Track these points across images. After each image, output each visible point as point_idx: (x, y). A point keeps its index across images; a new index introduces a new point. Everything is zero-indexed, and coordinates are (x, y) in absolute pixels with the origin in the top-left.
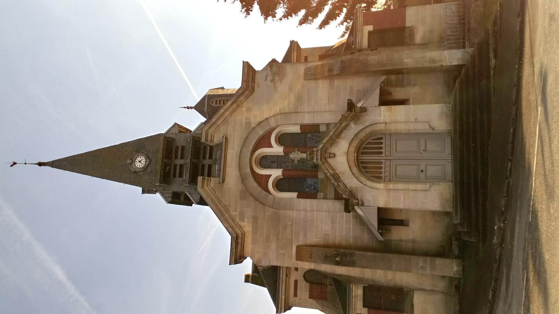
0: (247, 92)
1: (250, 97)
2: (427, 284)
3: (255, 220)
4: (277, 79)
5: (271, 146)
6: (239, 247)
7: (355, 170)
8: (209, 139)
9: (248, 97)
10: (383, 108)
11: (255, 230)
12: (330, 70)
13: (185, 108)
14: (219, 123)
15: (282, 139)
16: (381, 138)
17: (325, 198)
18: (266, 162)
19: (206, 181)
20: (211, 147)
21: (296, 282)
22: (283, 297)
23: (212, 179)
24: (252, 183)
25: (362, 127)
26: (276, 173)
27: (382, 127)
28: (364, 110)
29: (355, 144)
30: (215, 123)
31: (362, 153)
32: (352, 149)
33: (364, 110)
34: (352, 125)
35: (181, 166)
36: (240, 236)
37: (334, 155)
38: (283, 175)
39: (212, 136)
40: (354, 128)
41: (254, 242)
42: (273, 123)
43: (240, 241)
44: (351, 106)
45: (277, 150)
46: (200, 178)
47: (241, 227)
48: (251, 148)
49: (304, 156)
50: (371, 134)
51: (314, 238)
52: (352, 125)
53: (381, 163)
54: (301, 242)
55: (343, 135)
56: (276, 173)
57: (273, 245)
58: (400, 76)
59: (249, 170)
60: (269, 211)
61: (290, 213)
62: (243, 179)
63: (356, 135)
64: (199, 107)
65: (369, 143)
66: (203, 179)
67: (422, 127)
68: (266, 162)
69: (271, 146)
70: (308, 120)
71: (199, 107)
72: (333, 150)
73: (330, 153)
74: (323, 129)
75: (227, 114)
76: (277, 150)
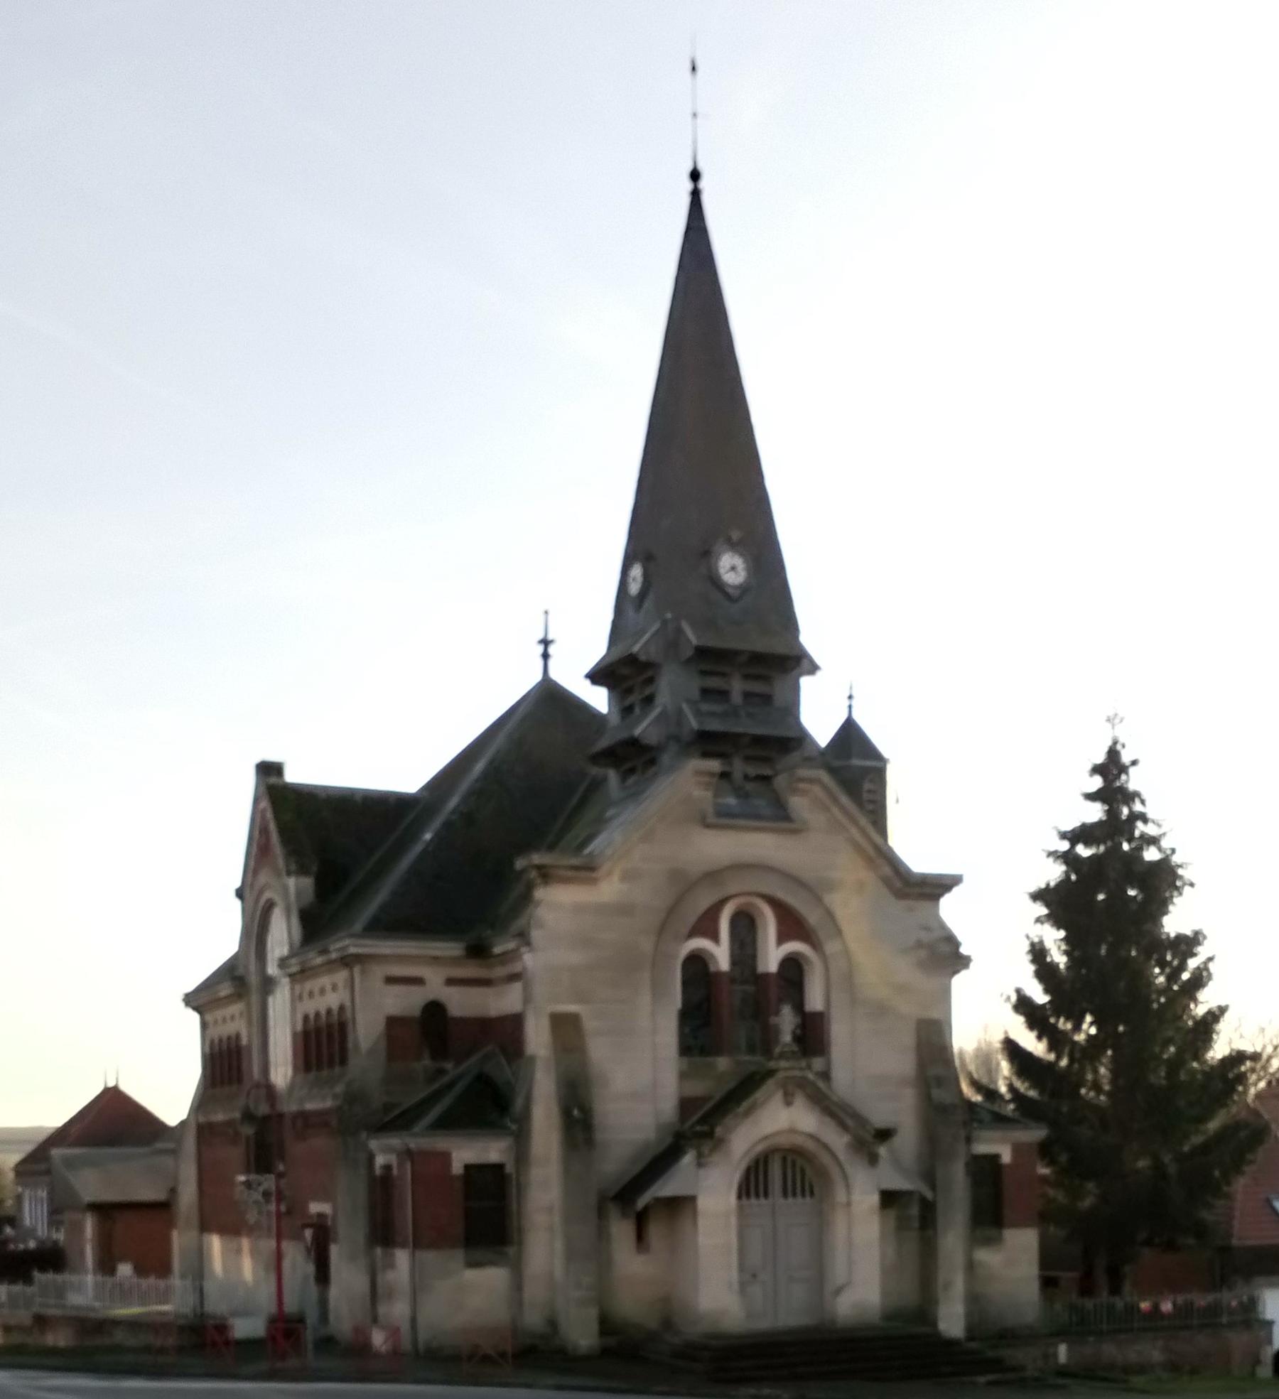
0: (898, 884)
1: (885, 891)
2: (534, 1292)
3: (623, 909)
4: (923, 953)
5: (781, 939)
6: (570, 873)
7: (760, 1148)
8: (801, 786)
9: (886, 882)
10: (875, 1199)
11: (602, 910)
12: (940, 1081)
13: (851, 688)
14: (835, 810)
15: (793, 969)
16: (812, 1193)
17: (683, 1076)
18: (745, 925)
19: (707, 779)
20: (766, 779)
21: (418, 981)
22: (387, 951)
23: (709, 794)
24: (703, 901)
25: (842, 1156)
26: (721, 955)
27: (841, 1196)
28: (873, 1160)
29: (810, 1145)
30: (835, 800)
31: (784, 1159)
32: (799, 1140)
33: (873, 1160)
34: (846, 1139)
35: (723, 695)
36: (594, 875)
37: (788, 1103)
38: (719, 974)
39: (804, 793)
40: (838, 1141)
41: (579, 909)
42: (831, 947)
43: (583, 874)
44: (885, 1135)
45: (772, 956)
46: (715, 765)
47: (609, 873)
48: (781, 895)
49: (787, 1037)
50: (823, 1174)
51: (599, 1050)
52: (846, 1139)
53: (766, 1195)
54: (589, 1024)
55: (828, 1119)
56: (721, 955)
57: (575, 957)
58: (916, 1224)
59: (732, 889)
60: (647, 945)
61: (645, 999)
62: (713, 876)
63: (826, 1147)
64: (850, 735)
65: (803, 1172)
66: (712, 774)
67: (838, 1271)
68: (745, 925)
69: (781, 939)
70: (839, 1032)
71: (850, 735)
72: (800, 1102)
73: (793, 1095)
74: (818, 1063)
75: (854, 832)
76: (772, 956)
